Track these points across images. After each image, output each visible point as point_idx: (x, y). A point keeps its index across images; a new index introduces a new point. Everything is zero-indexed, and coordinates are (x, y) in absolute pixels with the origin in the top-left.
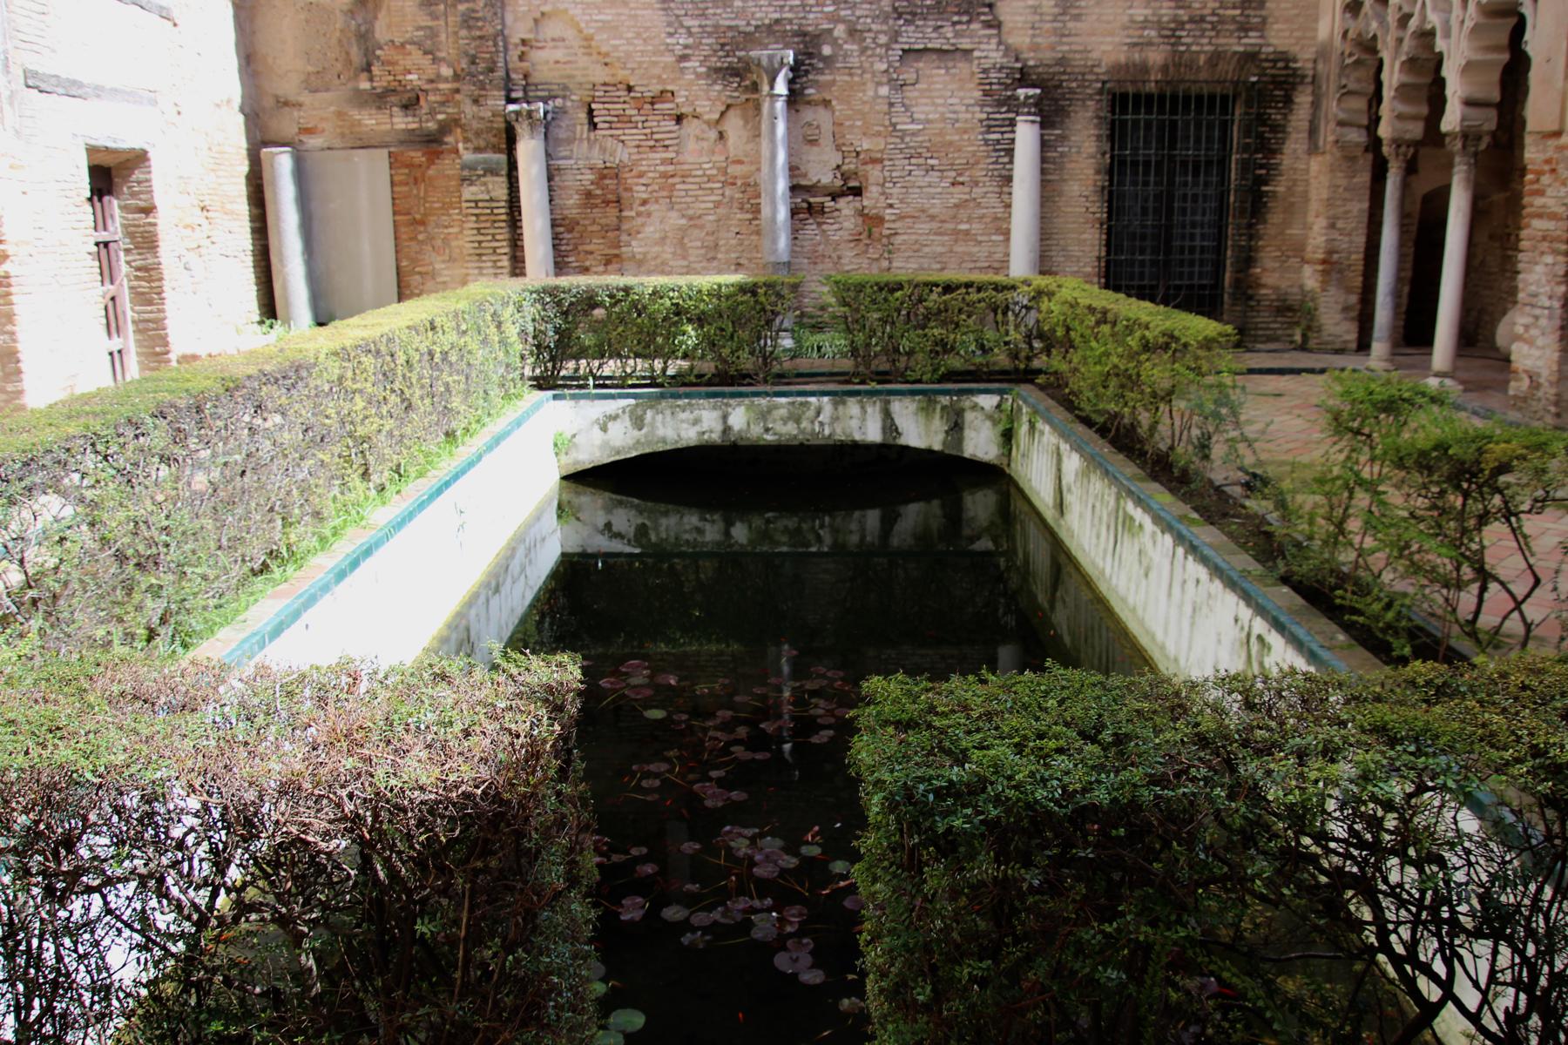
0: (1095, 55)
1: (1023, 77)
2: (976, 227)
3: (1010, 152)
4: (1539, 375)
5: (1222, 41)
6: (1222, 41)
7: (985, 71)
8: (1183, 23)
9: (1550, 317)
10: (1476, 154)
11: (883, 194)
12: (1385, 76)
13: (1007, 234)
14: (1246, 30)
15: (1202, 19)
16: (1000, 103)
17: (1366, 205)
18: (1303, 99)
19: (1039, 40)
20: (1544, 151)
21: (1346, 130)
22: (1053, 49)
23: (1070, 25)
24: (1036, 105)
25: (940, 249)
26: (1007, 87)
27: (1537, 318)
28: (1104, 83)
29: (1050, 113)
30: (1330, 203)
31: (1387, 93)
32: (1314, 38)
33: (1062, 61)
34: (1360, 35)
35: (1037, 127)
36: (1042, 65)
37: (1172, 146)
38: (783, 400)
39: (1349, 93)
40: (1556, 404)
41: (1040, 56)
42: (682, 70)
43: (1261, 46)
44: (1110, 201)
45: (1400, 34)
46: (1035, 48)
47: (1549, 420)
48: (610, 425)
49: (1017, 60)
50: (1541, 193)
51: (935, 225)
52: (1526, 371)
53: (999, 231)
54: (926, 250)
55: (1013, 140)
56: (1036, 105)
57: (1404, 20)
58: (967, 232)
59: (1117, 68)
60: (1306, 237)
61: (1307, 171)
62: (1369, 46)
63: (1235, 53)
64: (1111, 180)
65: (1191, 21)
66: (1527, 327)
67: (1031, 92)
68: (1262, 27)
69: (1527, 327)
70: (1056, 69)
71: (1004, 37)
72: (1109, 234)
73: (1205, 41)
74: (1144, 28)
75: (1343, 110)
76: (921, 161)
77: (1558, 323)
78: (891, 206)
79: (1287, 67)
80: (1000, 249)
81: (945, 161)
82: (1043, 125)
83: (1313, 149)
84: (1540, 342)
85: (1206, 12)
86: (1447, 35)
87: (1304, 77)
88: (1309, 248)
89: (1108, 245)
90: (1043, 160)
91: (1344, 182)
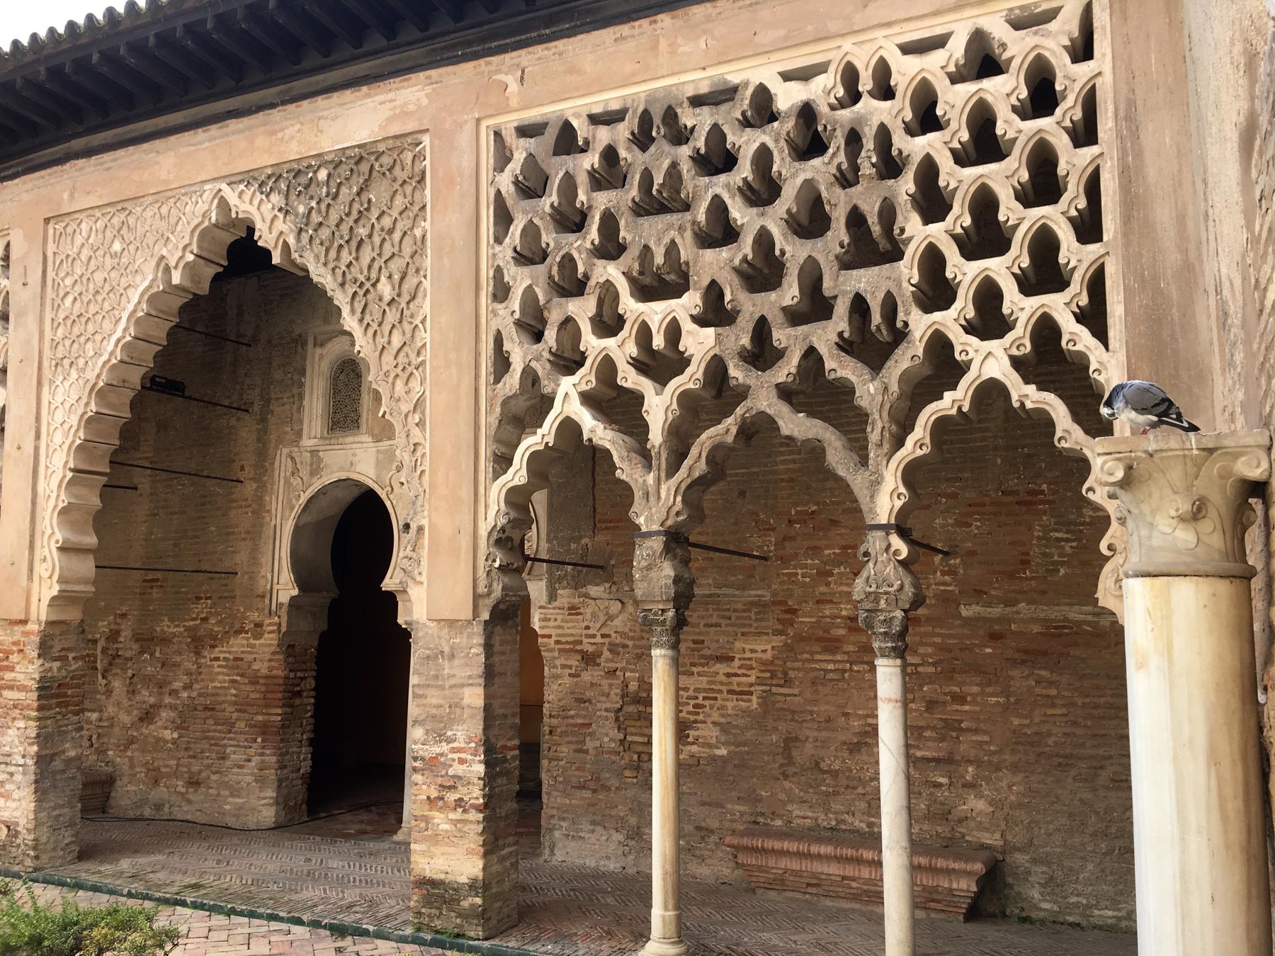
4: (17, 824)
9: (24, 774)
20: (12, 635)
27: (12, 774)
40: (35, 848)
47: (28, 862)
50: (12, 669)
77: (33, 777)
84: (15, 796)
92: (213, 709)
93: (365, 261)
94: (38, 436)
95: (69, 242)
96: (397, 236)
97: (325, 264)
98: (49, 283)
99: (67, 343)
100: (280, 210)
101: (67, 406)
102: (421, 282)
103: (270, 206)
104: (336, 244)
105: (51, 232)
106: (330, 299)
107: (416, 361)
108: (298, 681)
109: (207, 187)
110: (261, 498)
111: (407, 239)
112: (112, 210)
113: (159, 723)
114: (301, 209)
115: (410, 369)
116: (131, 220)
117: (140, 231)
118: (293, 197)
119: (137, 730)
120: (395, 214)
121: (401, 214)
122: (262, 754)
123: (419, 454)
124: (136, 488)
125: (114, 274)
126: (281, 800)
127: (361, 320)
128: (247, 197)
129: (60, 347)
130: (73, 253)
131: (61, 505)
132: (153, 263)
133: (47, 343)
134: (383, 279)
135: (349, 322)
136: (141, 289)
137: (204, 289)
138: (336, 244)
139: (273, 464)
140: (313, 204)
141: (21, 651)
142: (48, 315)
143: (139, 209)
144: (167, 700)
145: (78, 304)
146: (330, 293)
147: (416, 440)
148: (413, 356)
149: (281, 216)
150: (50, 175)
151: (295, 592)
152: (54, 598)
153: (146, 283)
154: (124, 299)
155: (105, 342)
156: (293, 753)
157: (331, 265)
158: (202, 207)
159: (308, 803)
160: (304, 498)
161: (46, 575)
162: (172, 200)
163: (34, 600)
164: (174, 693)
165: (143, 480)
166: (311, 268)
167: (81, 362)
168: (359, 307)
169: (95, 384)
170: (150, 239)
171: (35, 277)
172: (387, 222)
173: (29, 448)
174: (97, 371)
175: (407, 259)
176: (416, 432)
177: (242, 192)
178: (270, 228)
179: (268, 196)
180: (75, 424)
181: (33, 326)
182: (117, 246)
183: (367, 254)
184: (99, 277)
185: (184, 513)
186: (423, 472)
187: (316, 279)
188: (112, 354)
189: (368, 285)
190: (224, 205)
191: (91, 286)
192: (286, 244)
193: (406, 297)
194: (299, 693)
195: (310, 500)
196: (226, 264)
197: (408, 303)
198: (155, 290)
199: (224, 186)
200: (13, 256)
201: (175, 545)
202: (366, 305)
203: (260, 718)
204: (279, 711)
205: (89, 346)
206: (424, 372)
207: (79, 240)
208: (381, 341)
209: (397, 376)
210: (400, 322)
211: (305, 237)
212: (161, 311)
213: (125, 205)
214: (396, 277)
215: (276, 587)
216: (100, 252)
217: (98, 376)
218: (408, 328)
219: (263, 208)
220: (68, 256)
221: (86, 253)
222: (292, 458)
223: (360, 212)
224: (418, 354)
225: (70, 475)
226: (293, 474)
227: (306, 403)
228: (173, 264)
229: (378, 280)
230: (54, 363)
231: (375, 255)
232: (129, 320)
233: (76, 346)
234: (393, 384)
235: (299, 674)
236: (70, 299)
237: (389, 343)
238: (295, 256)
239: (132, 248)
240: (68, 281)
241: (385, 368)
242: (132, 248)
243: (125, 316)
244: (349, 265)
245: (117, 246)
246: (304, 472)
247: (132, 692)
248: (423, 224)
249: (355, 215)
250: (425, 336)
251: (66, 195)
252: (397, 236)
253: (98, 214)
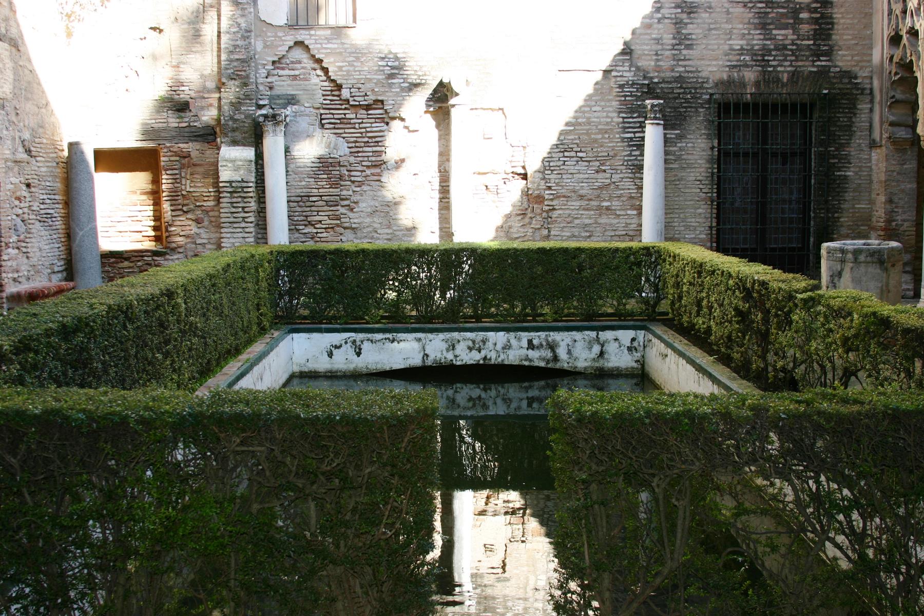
0: (703, 74)
1: (650, 91)
2: (616, 203)
3: (641, 147)
5: (800, 64)
6: (800, 64)
7: (621, 86)
8: (771, 50)
11: (544, 179)
13: (639, 209)
14: (818, 56)
15: (785, 47)
16: (632, 111)
18: (863, 106)
19: (661, 63)
21: (896, 129)
22: (673, 71)
23: (684, 52)
24: (660, 111)
25: (587, 221)
26: (638, 98)
28: (711, 95)
29: (673, 121)
30: (887, 183)
32: (870, 61)
33: (680, 79)
34: (901, 59)
35: (661, 128)
36: (664, 82)
37: (765, 142)
38: (469, 335)
39: (897, 102)
41: (662, 75)
42: (391, 85)
43: (829, 67)
44: (718, 185)
46: (658, 69)
48: (335, 352)
49: (645, 78)
51: (584, 203)
53: (633, 207)
54: (577, 222)
55: (643, 138)
56: (660, 111)
58: (608, 208)
59: (719, 83)
60: (871, 210)
61: (870, 160)
63: (811, 72)
64: (719, 168)
65: (777, 48)
67: (656, 102)
68: (829, 53)
70: (674, 85)
71: (634, 61)
72: (718, 209)
73: (788, 63)
74: (742, 54)
75: (893, 115)
76: (573, 154)
78: (549, 188)
79: (850, 83)
80: (633, 221)
81: (590, 154)
82: (665, 127)
83: (873, 145)
85: (787, 42)
87: (864, 89)
88: (874, 219)
89: (718, 218)
90: (667, 153)
91: (897, 168)
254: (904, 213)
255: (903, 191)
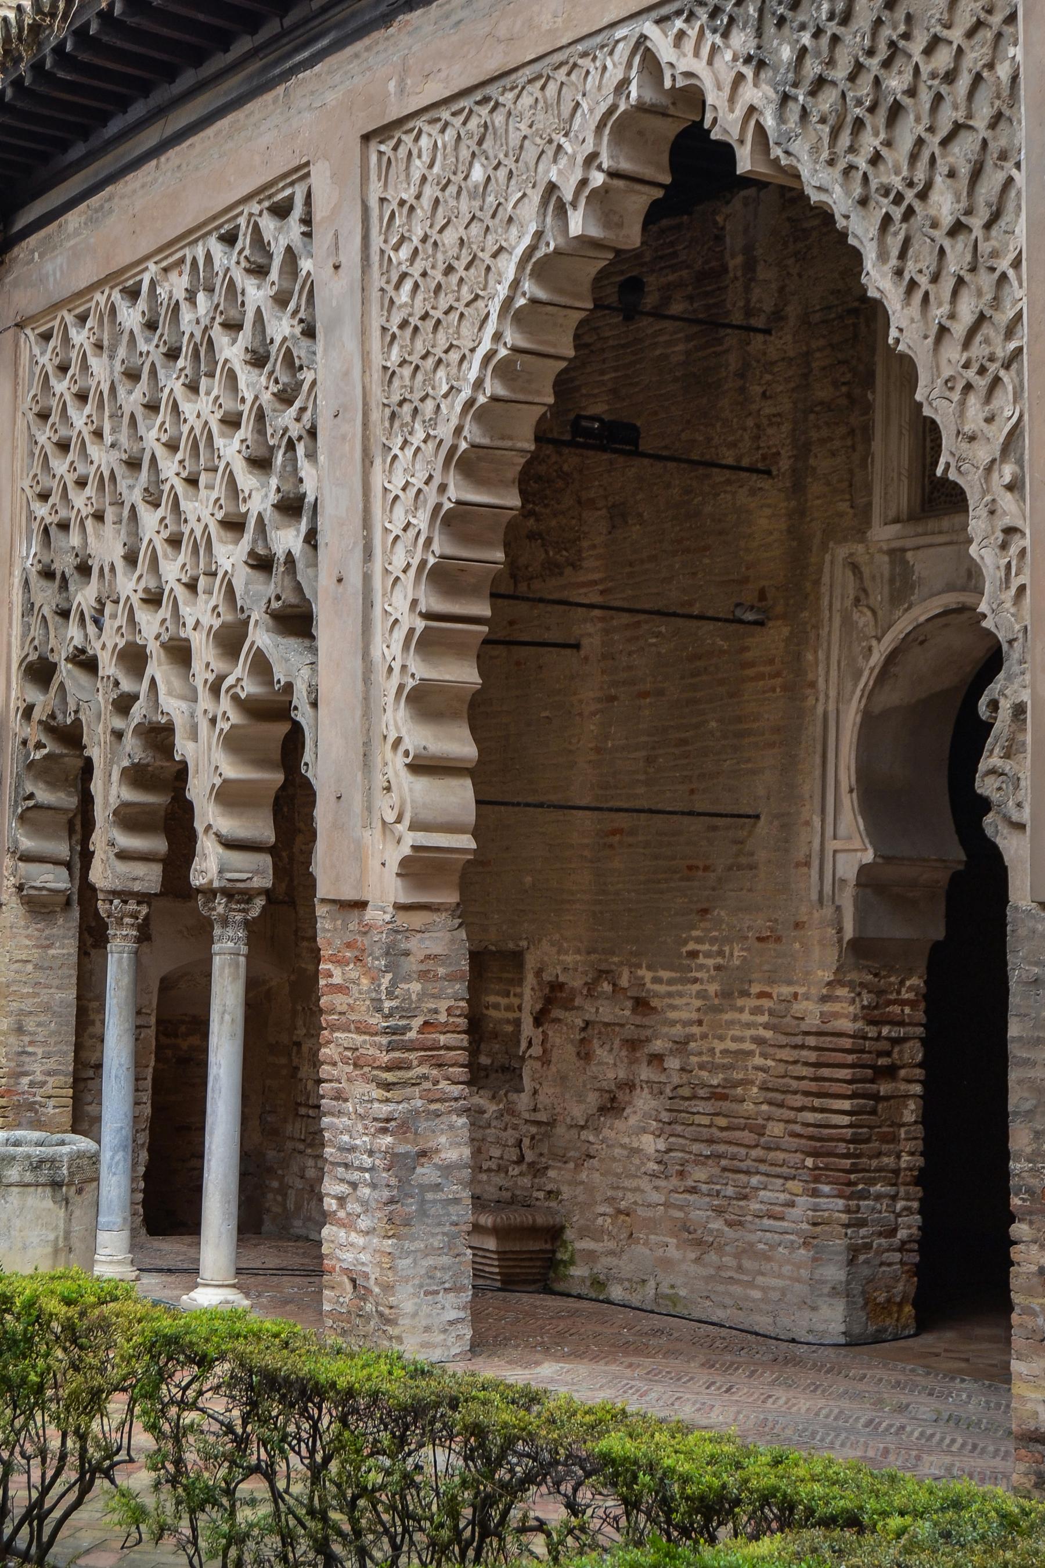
10: (247, 924)
12: (96, 787)
17: (71, 995)
31: (101, 814)
34: (53, 716)
45: (118, 723)
52: (346, 1271)
57: (124, 704)
62: (70, 736)
66: (342, 1200)
69: (342, 1200)
86: (194, 736)
92: (724, 1097)
93: (905, 144)
94: (368, 554)
95: (402, 177)
96: (964, 82)
97: (831, 163)
98: (375, 258)
99: (407, 371)
100: (748, 60)
101: (412, 492)
102: (1010, 180)
103: (728, 56)
104: (849, 119)
105: (374, 158)
106: (844, 235)
107: (1003, 349)
108: (884, 1045)
109: (620, 33)
110: (798, 657)
111: (984, 94)
112: (466, 103)
113: (633, 1121)
114: (786, 53)
115: (992, 368)
116: (499, 118)
117: (514, 139)
118: (770, 30)
119: (597, 1130)
120: (956, 35)
121: (970, 34)
122: (815, 1193)
123: (1013, 550)
124: (577, 646)
125: (476, 229)
126: (856, 1288)
127: (899, 273)
128: (689, 45)
129: (396, 383)
130: (408, 196)
131: (411, 683)
132: (535, 197)
133: (376, 375)
134: (938, 179)
135: (878, 279)
136: (519, 251)
137: (632, 236)
138: (849, 119)
139: (817, 582)
140: (806, 39)
141: (358, 959)
142: (376, 321)
143: (510, 96)
144: (645, 1073)
145: (420, 296)
146: (841, 223)
147: (1007, 521)
148: (997, 338)
149: (748, 71)
150: (368, 49)
151: (868, 857)
152: (405, 862)
153: (527, 241)
154: (492, 278)
155: (465, 365)
156: (878, 1197)
157: (842, 165)
158: (614, 75)
159: (918, 1303)
160: (877, 658)
161: (390, 817)
162: (564, 70)
163: (374, 864)
164: (657, 1059)
165: (589, 628)
166: (805, 173)
167: (429, 406)
168: (894, 245)
169: (454, 448)
170: (530, 153)
171: (351, 253)
172: (943, 59)
173: (354, 579)
174: (454, 422)
175: (983, 133)
176: (1007, 501)
177: (681, 35)
178: (732, 100)
179: (725, 35)
180: (424, 526)
181: (351, 344)
182: (478, 174)
183: (908, 132)
184: (450, 238)
185: (660, 693)
186: (1022, 589)
187: (815, 197)
188: (478, 384)
189: (910, 195)
190: (651, 65)
191: (440, 257)
192: (760, 128)
193: (983, 215)
194: (890, 1072)
195: (891, 658)
196: (667, 179)
197: (988, 226)
198: (539, 254)
199: (649, 28)
200: (318, 216)
201: (649, 760)
202: (907, 243)
203: (810, 1117)
204: (846, 1105)
205: (441, 373)
206: (1020, 373)
207: (418, 166)
208: (939, 312)
209: (968, 387)
210: (973, 269)
211: (793, 112)
212: (561, 291)
213: (489, 90)
214: (964, 171)
215: (831, 845)
216: (452, 189)
217: (458, 431)
218: (986, 281)
219: (718, 62)
220: (402, 203)
221: (430, 192)
222: (855, 568)
223: (892, 44)
224: (1010, 333)
225: (420, 624)
226: (857, 601)
227: (877, 446)
228: (568, 196)
229: (929, 185)
230: (387, 412)
231: (920, 130)
232: (501, 315)
233: (420, 377)
234: (963, 403)
235: (885, 1031)
236: (408, 286)
237: (952, 316)
238: (776, 152)
239: (502, 173)
240: (404, 253)
241: (947, 373)
242: (502, 173)
243: (495, 307)
244: (876, 159)
245: (478, 174)
246: (879, 596)
247: (585, 1056)
248: (1011, 51)
249: (883, 52)
250: (1018, 294)
251: (392, 86)
252: (964, 82)
253: (445, 115)
254: (47, 1056)
255: (47, 1008)
